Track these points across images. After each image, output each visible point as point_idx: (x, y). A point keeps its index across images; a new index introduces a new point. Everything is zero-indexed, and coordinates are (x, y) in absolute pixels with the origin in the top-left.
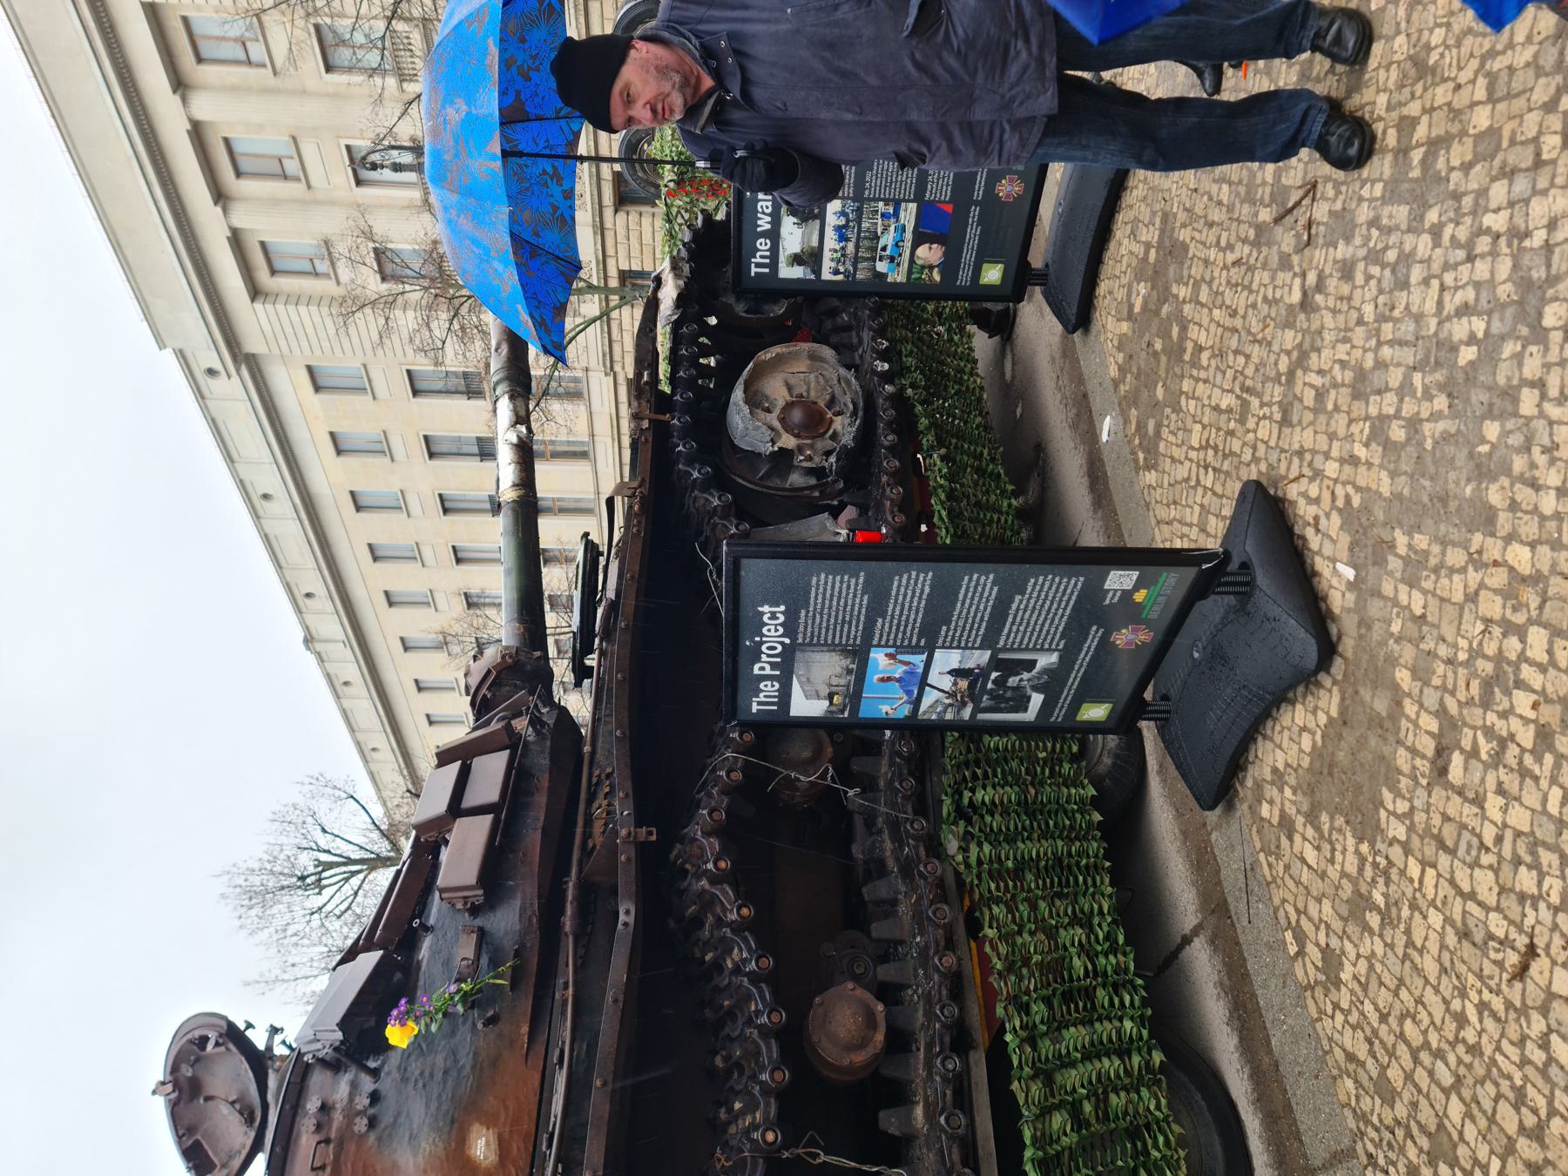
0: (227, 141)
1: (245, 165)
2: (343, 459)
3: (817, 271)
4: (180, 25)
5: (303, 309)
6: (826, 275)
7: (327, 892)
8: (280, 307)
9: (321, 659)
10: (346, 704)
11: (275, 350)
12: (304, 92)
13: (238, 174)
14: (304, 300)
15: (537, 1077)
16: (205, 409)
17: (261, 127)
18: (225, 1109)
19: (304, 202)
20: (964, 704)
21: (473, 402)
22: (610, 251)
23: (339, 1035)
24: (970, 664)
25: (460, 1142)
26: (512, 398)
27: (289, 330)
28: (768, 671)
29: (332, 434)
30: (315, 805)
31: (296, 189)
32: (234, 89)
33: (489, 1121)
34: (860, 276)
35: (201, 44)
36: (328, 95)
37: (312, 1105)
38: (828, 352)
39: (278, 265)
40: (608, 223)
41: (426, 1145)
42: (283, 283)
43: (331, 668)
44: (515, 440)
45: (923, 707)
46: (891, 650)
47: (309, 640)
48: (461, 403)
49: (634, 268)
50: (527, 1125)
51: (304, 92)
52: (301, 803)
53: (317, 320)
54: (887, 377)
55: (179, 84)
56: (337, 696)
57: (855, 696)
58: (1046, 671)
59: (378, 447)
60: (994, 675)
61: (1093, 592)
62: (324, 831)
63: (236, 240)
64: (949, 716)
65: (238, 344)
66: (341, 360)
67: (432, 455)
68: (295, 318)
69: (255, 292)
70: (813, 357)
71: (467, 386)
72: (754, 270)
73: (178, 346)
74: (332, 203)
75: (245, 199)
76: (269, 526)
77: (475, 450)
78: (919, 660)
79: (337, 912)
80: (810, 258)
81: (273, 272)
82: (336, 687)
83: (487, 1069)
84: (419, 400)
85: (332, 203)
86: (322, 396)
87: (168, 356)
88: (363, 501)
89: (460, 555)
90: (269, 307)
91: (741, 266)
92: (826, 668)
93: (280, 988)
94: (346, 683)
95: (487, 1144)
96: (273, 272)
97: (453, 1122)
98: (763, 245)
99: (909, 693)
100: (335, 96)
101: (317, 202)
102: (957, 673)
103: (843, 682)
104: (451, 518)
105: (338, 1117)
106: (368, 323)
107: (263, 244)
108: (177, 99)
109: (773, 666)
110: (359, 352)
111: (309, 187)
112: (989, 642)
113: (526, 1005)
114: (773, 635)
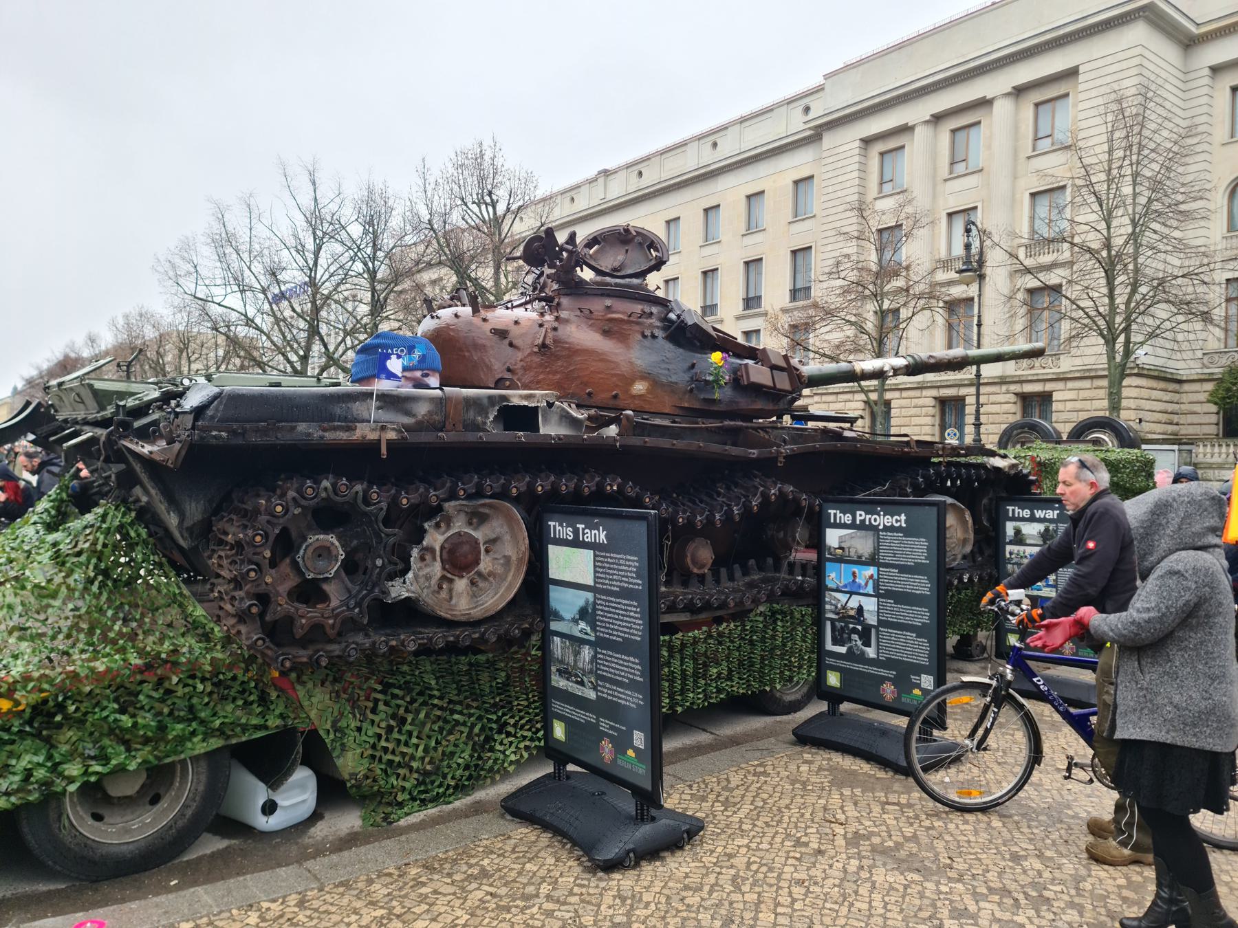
0: (979, 123)
1: (961, 136)
2: (744, 200)
3: (1011, 543)
4: (1062, 91)
5: (856, 174)
6: (1009, 548)
7: (475, 208)
8: (857, 159)
9: (591, 181)
11: (825, 154)
12: (1015, 178)
13: (954, 131)
14: (863, 175)
16: (780, 105)
17: (989, 147)
18: (621, 258)
19: (934, 177)
20: (837, 614)
21: (788, 293)
22: (905, 394)
24: (866, 615)
27: (840, 164)
28: (858, 519)
29: (763, 192)
31: (944, 171)
32: (1016, 128)
34: (1009, 567)
35: (1048, 106)
36: (1013, 195)
37: (655, 310)
38: (968, 549)
39: (886, 157)
40: (926, 393)
41: (639, 362)
42: (874, 162)
43: (585, 189)
45: (833, 594)
46: (875, 577)
47: (606, 173)
48: (787, 286)
49: (893, 412)
50: (647, 407)
51: (1015, 178)
53: (848, 184)
54: (961, 580)
55: (1019, 91)
57: (840, 560)
58: (863, 653)
59: (753, 224)
60: (859, 628)
61: (919, 670)
63: (906, 129)
64: (828, 607)
65: (829, 129)
66: (817, 200)
67: (747, 263)
68: (849, 169)
69: (867, 142)
70: (965, 541)
71: (800, 290)
72: (1010, 508)
73: (826, 86)
74: (934, 196)
75: (935, 136)
76: (692, 149)
77: (752, 295)
78: (870, 590)
79: (467, 217)
80: (1019, 539)
81: (882, 154)
83: (671, 388)
84: (789, 256)
85: (934, 196)
86: (791, 186)
87: (819, 80)
88: (712, 214)
89: (671, 283)
90: (857, 151)
91: (1013, 501)
92: (863, 545)
93: (421, 182)
94: (573, 199)
96: (882, 154)
98: (1026, 513)
99: (845, 586)
101: (934, 186)
102: (860, 610)
103: (852, 554)
104: (700, 276)
106: (850, 223)
107: (903, 147)
108: (1009, 90)
109: (863, 521)
111: (946, 180)
112: (881, 623)
113: (697, 405)
114: (883, 520)
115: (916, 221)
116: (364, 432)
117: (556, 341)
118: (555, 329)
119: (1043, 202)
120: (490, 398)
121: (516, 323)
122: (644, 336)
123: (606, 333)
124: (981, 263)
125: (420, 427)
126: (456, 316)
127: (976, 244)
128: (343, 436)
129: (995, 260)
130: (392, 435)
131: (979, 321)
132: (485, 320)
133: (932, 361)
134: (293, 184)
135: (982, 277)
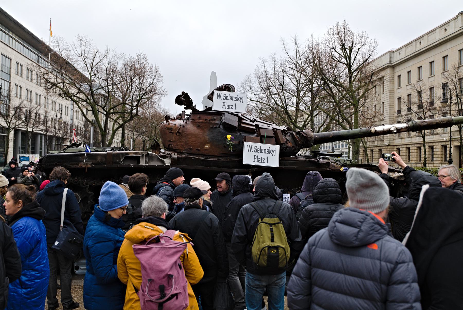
9: (455, 19)
10: (438, 31)
15: (216, 155)
26: (406, 127)
30: (368, 44)
33: (211, 147)
37: (215, 118)
52: (368, 40)
56: (440, 27)
62: (359, 49)
82: (444, 26)
94: (446, 29)
105: (213, 122)
116: (82, 165)
117: (183, 131)
118: (184, 126)
123: (198, 127)
125: (98, 163)
128: (76, 166)
130: (89, 166)
133: (425, 124)
134: (287, 48)
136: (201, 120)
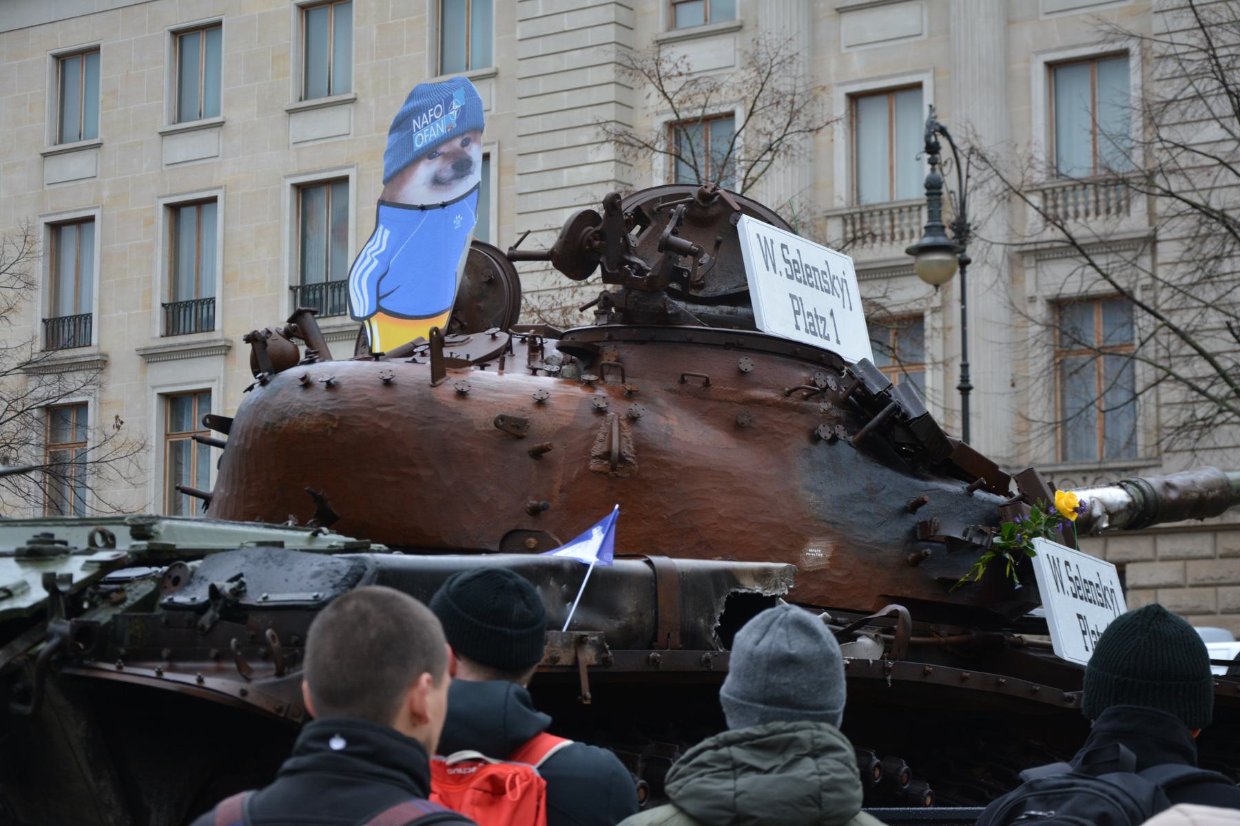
12: (1010, 22)
23: (914, 414)
25: (824, 533)
26: (1130, 507)
44: (1097, 511)
51: (1010, 22)
95: (818, 559)
97: (833, 523)
100: (1008, 76)
101: (814, 21)
104: (161, 219)
110: (525, 69)
115: (793, 114)
117: (641, 448)
119: (1077, 86)
120: (716, 575)
121: (541, 403)
122: (815, 438)
124: (962, 230)
126: (388, 383)
127: (951, 182)
129: (991, 224)
131: (965, 378)
132: (461, 394)
133: (1173, 495)
135: (964, 263)
136: (756, 385)
